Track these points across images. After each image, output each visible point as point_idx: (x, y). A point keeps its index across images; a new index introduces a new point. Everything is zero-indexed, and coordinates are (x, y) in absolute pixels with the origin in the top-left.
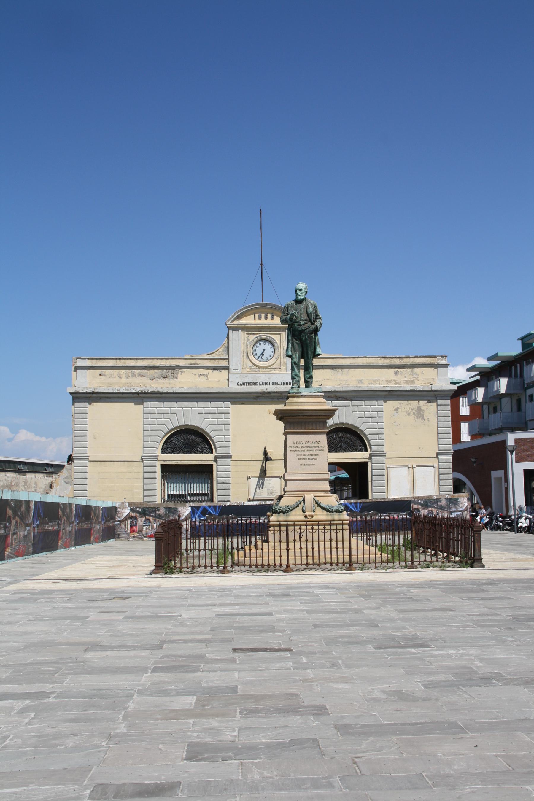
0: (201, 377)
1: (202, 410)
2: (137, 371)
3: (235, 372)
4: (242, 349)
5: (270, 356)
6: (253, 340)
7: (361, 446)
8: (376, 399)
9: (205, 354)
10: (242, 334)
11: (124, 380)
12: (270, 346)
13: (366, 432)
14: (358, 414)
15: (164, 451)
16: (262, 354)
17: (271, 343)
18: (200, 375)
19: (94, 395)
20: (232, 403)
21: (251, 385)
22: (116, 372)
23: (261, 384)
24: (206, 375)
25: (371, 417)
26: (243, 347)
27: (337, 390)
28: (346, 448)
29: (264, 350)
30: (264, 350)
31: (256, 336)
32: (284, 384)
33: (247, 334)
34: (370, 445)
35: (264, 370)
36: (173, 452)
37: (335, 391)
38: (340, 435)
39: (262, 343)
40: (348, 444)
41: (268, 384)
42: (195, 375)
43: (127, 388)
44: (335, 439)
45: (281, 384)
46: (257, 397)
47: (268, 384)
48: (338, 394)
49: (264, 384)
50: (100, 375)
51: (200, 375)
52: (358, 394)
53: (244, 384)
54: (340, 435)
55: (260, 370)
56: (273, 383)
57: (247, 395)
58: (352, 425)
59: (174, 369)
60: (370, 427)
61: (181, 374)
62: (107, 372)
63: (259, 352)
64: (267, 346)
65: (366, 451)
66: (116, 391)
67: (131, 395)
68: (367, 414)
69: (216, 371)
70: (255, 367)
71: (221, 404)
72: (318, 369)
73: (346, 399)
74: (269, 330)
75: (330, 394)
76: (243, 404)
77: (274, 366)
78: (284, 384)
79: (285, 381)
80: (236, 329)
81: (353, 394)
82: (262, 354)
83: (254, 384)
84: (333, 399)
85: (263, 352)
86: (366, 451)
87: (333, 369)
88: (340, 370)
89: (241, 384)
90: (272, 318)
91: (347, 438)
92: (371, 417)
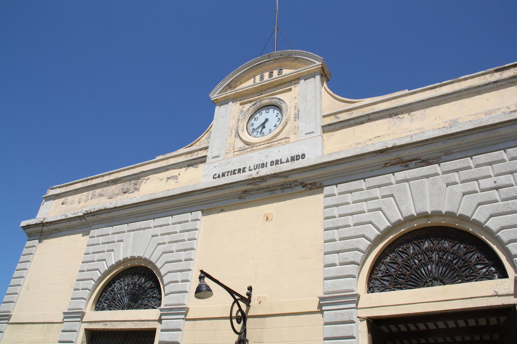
0: (170, 181)
1: (159, 231)
2: (98, 191)
3: (214, 160)
4: (230, 126)
5: (275, 126)
6: (248, 110)
7: (486, 265)
8: (501, 146)
9: (182, 149)
10: (234, 107)
11: (83, 204)
12: (276, 111)
13: (493, 224)
14: (460, 188)
15: (99, 305)
16: (263, 126)
17: (277, 107)
18: (169, 178)
19: (45, 228)
20: (205, 212)
21: (234, 173)
22: (76, 197)
23: (252, 168)
24: (175, 177)
25: (497, 188)
26: (232, 123)
27: (399, 143)
28: (443, 274)
29: (267, 120)
30: (267, 120)
31: (254, 103)
32: (293, 159)
33: (241, 104)
34: (510, 257)
35: (261, 147)
36: (110, 308)
37: (395, 148)
38: (426, 245)
39: (264, 112)
40: (448, 265)
41: (263, 165)
42: (162, 180)
43: (76, 212)
44: (413, 258)
45: (287, 161)
46: (245, 192)
47: (263, 165)
48: (405, 154)
49: (256, 167)
50: (63, 204)
51: (169, 178)
52: (450, 144)
53: (223, 175)
54: (426, 245)
55: (254, 148)
56: (272, 162)
57: (227, 191)
58: (450, 215)
59: (139, 178)
60: (500, 211)
61: (145, 183)
62: (70, 198)
63: (257, 124)
64: (272, 115)
65: (504, 275)
66: (64, 217)
67: (78, 222)
68: (485, 183)
69: (191, 168)
70: (247, 146)
71: (188, 216)
72: (362, 123)
73: (426, 162)
74: (274, 89)
75: (386, 158)
76: (222, 211)
77: (280, 137)
78: (293, 159)
79: (294, 154)
80: (224, 102)
81: (440, 146)
82: (263, 126)
83: (239, 170)
84: (398, 167)
85: (264, 123)
86: (504, 275)
87: (390, 116)
88: (406, 115)
89: (219, 176)
90: (280, 73)
91: (445, 251)
92: (497, 188)
